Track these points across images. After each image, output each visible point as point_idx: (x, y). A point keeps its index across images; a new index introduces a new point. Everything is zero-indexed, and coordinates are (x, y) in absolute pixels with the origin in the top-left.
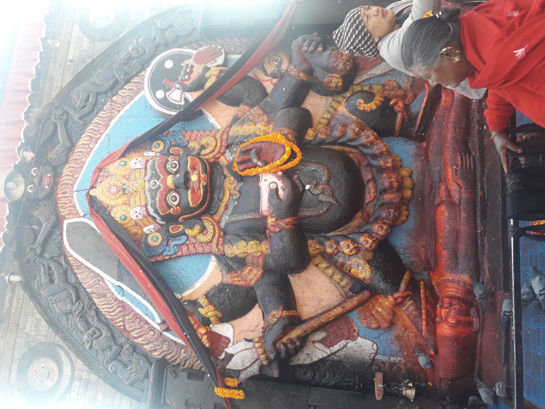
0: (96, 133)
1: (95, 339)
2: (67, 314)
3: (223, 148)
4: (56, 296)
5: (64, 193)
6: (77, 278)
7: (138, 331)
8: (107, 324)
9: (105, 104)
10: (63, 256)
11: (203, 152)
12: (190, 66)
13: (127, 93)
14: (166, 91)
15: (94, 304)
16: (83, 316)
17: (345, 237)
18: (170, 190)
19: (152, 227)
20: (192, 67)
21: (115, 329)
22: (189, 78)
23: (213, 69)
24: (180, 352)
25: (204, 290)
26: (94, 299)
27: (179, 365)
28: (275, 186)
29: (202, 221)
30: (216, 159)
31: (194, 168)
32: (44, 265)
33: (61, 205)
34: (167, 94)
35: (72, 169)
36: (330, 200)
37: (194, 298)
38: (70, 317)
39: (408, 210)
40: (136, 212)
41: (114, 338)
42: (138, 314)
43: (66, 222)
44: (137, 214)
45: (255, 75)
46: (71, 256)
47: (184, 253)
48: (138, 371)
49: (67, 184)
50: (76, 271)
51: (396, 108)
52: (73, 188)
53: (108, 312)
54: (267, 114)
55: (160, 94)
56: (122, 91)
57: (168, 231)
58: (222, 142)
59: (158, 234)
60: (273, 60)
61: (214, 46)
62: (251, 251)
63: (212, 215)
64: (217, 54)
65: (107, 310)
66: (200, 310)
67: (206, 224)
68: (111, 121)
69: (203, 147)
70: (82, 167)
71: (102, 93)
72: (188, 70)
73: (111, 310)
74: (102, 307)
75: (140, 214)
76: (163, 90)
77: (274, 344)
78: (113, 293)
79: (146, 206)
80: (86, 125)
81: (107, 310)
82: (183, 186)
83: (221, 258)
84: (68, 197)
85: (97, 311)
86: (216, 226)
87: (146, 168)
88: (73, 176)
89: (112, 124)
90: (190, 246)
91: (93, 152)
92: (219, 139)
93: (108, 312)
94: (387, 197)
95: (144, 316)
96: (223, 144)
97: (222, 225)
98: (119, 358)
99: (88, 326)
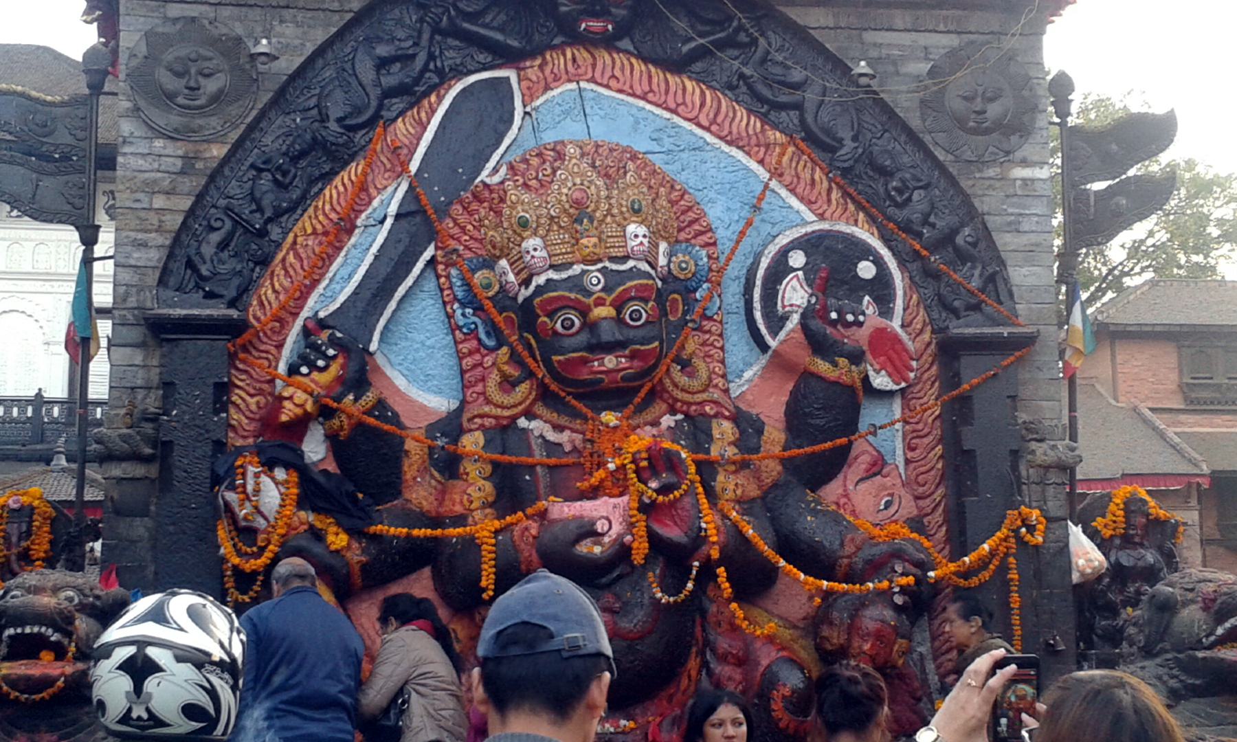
0: (711, 115)
1: (273, 176)
3: (685, 408)
4: (355, 83)
5: (574, 60)
6: (395, 120)
7: (298, 266)
10: (437, 80)
12: (861, 318)
15: (346, 164)
16: (317, 144)
18: (584, 312)
19: (511, 277)
21: (295, 216)
24: (260, 358)
26: (354, 164)
28: (601, 526)
31: (633, 356)
32: (416, 44)
33: (548, 57)
34: (800, 273)
35: (628, 72)
37: (372, 377)
38: (315, 112)
40: (535, 250)
41: (278, 214)
42: (331, 264)
43: (511, 74)
44: (532, 253)
45: (856, 458)
46: (440, 99)
47: (461, 346)
48: (218, 277)
49: (594, 66)
50: (409, 113)
52: (588, 81)
53: (331, 197)
54: (763, 498)
55: (797, 259)
56: (809, 165)
59: (497, 288)
60: (889, 495)
61: (914, 364)
64: (897, 372)
65: (335, 196)
66: (351, 397)
67: (523, 388)
68: (739, 147)
69: (685, 364)
70: (634, 95)
71: (802, 121)
72: (850, 318)
73: (335, 202)
74: (340, 184)
75: (533, 257)
76: (807, 264)
78: (370, 203)
79: (552, 267)
81: (335, 196)
82: (594, 341)
84: (567, 72)
86: (520, 408)
87: (625, 258)
88: (613, 76)
89: (734, 152)
90: (477, 357)
91: (667, 115)
92: (704, 396)
93: (331, 197)
95: (330, 275)
96: (694, 408)
97: (522, 422)
98: (240, 231)
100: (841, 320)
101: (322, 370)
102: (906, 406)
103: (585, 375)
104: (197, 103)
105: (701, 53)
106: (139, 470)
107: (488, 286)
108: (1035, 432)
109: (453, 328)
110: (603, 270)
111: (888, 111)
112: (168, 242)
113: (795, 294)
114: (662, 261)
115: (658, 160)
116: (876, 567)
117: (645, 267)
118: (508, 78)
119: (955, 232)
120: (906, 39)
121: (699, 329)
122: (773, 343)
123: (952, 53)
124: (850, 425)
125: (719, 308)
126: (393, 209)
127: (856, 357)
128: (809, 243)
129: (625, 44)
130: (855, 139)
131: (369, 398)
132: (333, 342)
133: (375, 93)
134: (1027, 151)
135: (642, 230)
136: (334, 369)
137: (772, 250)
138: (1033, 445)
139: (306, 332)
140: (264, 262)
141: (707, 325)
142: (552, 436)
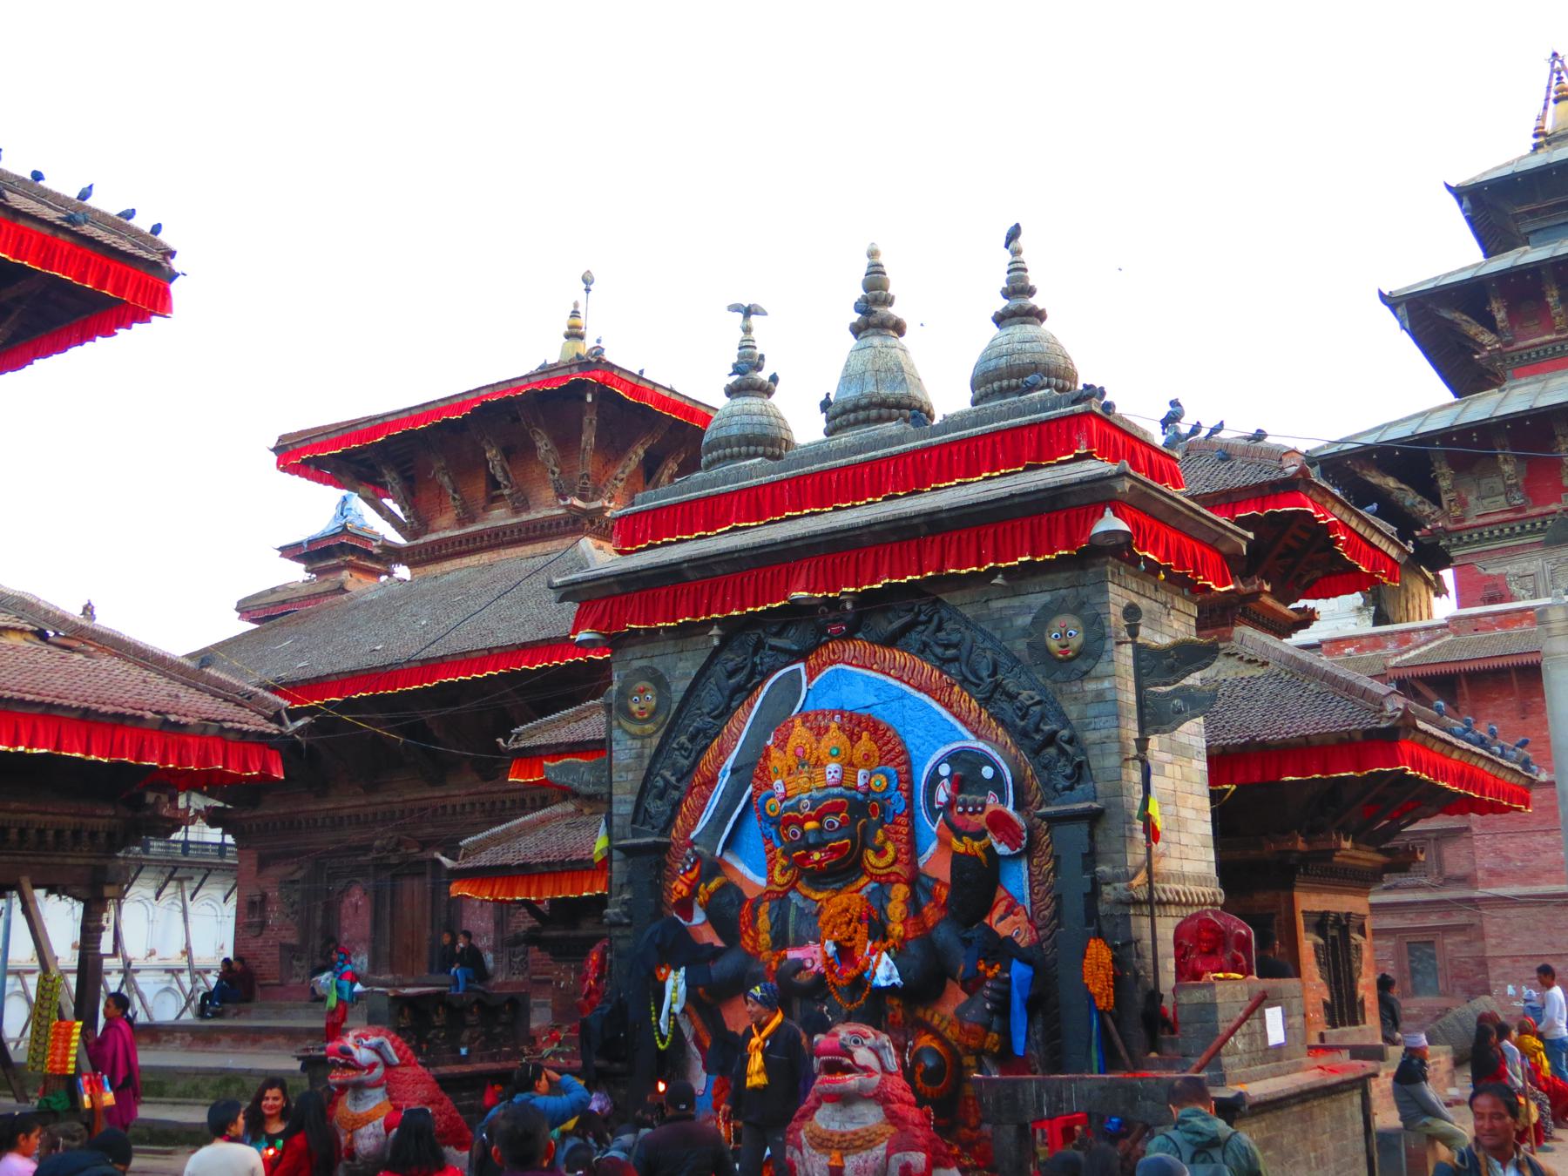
8: (695, 763)
9: (949, 674)
11: (870, 856)
14: (950, 777)
20: (981, 813)
23: (976, 844)
25: (735, 879)
27: (666, 864)
28: (809, 964)
30: (864, 871)
37: (726, 871)
43: (801, 666)
55: (945, 770)
58: (888, 874)
62: (761, 938)
64: (1012, 843)
67: (789, 873)
79: (786, 798)
83: (767, 895)
85: (706, 747)
89: (922, 696)
100: (965, 810)
101: (691, 870)
102: (1030, 862)
106: (628, 932)
110: (810, 798)
111: (1009, 654)
113: (942, 795)
114: (860, 782)
117: (836, 790)
119: (1056, 732)
120: (1016, 602)
121: (894, 822)
123: (1045, 607)
128: (953, 758)
129: (860, 635)
130: (994, 674)
131: (713, 885)
133: (727, 693)
134: (1101, 668)
137: (930, 764)
140: (676, 806)
141: (900, 819)
142: (801, 904)
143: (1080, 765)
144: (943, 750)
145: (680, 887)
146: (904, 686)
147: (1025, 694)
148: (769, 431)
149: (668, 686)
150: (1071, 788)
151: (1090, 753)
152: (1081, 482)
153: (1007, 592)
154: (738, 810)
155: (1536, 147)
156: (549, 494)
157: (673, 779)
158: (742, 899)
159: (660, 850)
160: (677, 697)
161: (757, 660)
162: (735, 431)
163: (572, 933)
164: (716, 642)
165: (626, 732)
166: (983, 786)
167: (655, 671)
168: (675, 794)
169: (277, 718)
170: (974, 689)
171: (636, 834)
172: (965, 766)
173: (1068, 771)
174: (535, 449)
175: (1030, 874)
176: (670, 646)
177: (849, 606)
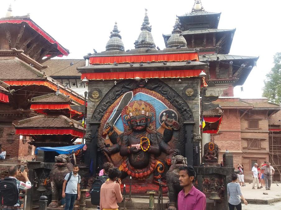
2: (109, 97)
13: (167, 103)
17: (127, 165)
20: (172, 122)
22: (168, 122)
25: (116, 131)
28: (137, 147)
29: (131, 129)
30: (147, 131)
31: (142, 127)
36: (135, 161)
39: (135, 180)
41: (104, 110)
43: (132, 92)
51: (159, 176)
55: (164, 114)
57: (128, 121)
63: (132, 131)
69: (150, 127)
77: (104, 150)
80: (158, 92)
85: (110, 105)
89: (158, 100)
94: (137, 174)
99: (107, 103)
103: (136, 129)
104: (96, 98)
105: (155, 88)
107: (127, 118)
108: (194, 136)
109: (123, 123)
112: (92, 114)
114: (147, 115)
115: (149, 102)
116: (172, 152)
118: (131, 92)
120: (180, 85)
121: (153, 123)
122: (161, 124)
124: (172, 135)
125: (155, 120)
126: (117, 109)
127: (171, 126)
128: (165, 112)
129: (146, 87)
132: (109, 125)
134: (196, 98)
135: (144, 111)
136: (109, 129)
137: (161, 113)
138: (195, 137)
139: (106, 124)
143: (191, 115)
144: (164, 111)
145: (105, 132)
146: (155, 98)
147: (180, 102)
148: (122, 45)
149: (102, 93)
150: (189, 119)
151: (193, 113)
152: (199, 65)
153: (180, 83)
154: (118, 118)
155: (193, 12)
156: (7, 46)
157: (102, 111)
158: (118, 135)
159: (99, 125)
160: (104, 95)
161: (123, 89)
162: (116, 44)
163: (44, 143)
164: (116, 84)
165: (91, 101)
166: (172, 117)
167: (99, 89)
168: (103, 114)
169: (7, 89)
170: (169, 100)
171: (92, 121)
172: (169, 114)
173: (189, 116)
174: (6, 35)
175: (179, 134)
176: (103, 85)
177: (146, 82)
